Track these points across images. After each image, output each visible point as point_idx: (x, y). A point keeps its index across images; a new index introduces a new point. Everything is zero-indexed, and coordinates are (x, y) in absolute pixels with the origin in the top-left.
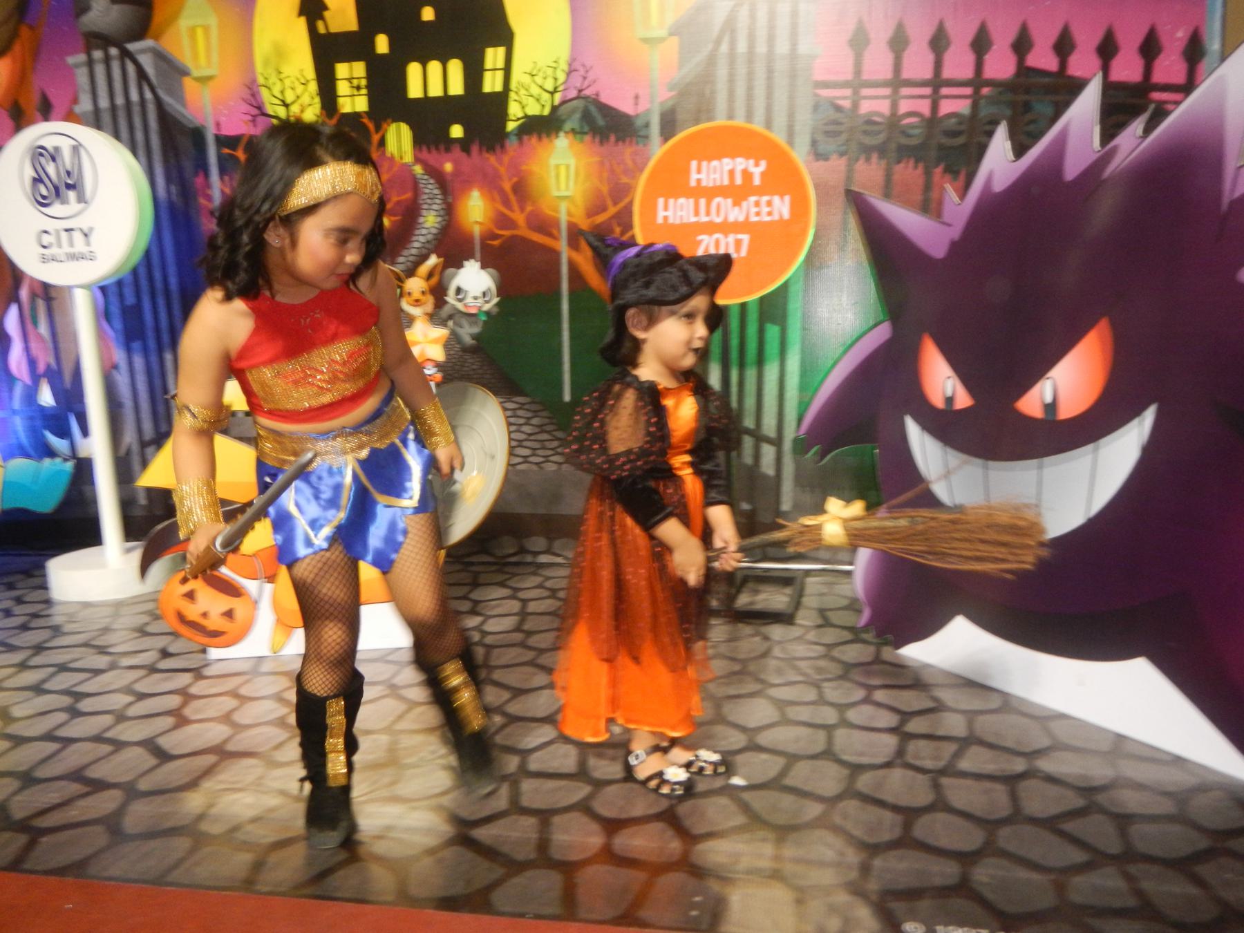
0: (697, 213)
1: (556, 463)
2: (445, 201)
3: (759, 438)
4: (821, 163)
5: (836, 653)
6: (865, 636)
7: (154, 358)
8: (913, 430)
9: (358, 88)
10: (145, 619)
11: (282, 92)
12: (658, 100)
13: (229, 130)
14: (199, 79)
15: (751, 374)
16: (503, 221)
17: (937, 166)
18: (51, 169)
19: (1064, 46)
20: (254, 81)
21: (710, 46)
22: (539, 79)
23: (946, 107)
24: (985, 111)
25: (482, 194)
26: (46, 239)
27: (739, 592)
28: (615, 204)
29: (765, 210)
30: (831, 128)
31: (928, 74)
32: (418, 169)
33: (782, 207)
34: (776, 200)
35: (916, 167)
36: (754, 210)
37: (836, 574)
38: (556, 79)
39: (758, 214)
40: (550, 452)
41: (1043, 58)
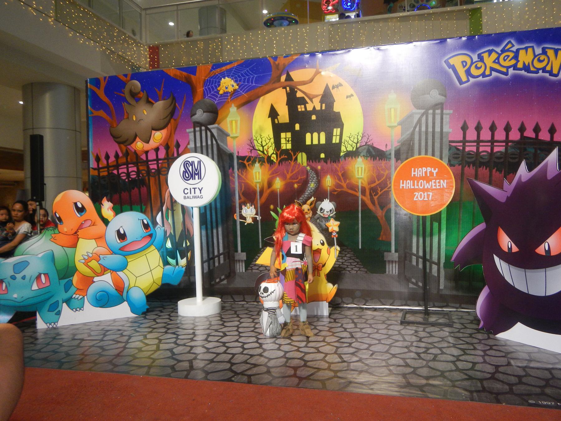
0: (414, 185)
1: (355, 270)
2: (317, 179)
3: (432, 263)
4: (452, 167)
5: (473, 336)
6: (481, 331)
7: (209, 232)
8: (496, 259)
9: (288, 141)
10: (221, 323)
11: (262, 142)
12: (394, 146)
13: (240, 155)
14: (232, 137)
15: (428, 240)
16: (338, 186)
17: (494, 169)
18: (190, 168)
19: (537, 129)
20: (252, 138)
21: (412, 129)
22: (352, 139)
23: (496, 149)
24: (510, 151)
25: (331, 177)
26: (186, 191)
27: (428, 318)
28: (378, 181)
29: (438, 184)
30: (456, 156)
31: (490, 139)
32: (308, 168)
33: (444, 183)
34: (442, 181)
35: (486, 169)
36: (433, 184)
37: (461, 312)
38: (358, 139)
39: (435, 186)
40: (354, 267)
41: (529, 133)
